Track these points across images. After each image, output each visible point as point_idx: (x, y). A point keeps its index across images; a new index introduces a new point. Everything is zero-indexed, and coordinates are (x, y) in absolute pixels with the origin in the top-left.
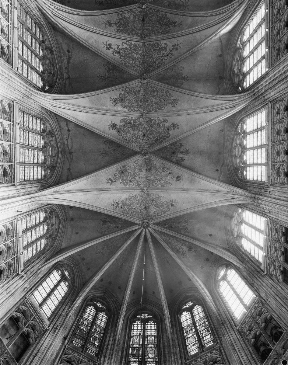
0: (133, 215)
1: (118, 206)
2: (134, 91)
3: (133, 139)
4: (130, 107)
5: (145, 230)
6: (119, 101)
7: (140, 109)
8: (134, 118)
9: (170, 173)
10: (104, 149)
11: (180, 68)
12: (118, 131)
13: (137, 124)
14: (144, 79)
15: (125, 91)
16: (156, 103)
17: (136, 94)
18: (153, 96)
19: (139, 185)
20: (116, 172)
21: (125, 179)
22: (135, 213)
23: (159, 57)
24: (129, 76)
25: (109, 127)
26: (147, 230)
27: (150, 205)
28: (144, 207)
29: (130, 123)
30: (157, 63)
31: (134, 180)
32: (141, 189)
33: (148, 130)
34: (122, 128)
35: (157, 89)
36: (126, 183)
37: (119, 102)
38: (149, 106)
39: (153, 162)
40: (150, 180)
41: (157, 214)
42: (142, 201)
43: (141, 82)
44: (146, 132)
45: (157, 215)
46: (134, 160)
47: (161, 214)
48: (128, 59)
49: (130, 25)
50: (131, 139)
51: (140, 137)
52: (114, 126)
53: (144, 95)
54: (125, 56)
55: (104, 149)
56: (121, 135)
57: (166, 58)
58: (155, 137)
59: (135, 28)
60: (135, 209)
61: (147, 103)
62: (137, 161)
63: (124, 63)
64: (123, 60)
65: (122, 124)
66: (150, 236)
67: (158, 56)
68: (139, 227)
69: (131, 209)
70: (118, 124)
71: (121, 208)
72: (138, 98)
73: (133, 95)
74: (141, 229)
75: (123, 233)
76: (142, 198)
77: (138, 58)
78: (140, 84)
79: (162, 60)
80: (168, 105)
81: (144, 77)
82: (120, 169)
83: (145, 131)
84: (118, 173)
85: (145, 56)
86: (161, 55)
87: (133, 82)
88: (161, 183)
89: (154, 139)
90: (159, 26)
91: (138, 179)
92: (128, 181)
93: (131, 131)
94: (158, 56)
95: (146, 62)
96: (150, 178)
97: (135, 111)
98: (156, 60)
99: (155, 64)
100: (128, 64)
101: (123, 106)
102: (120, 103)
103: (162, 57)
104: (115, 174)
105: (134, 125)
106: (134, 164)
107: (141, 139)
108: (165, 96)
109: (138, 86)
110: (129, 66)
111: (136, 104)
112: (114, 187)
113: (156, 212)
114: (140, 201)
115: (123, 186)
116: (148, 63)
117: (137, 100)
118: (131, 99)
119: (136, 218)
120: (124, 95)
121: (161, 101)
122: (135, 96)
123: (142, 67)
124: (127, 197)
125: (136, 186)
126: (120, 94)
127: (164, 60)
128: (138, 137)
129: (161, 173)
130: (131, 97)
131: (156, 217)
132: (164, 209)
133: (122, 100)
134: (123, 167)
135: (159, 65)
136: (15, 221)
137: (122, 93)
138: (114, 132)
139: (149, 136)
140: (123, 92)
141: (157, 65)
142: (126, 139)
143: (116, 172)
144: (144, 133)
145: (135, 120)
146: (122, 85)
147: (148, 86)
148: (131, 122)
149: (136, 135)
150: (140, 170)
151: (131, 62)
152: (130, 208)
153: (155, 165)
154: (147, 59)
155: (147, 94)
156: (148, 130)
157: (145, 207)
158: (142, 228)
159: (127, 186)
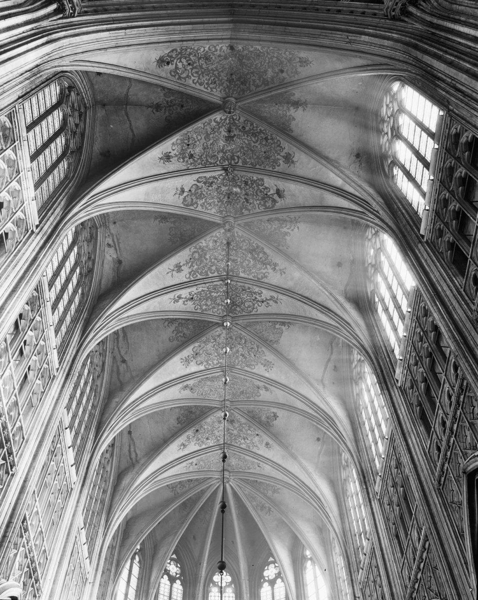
7: (221, 361)
9: (257, 435)
16: (243, 355)
17: (215, 340)
18: (239, 344)
36: (202, 442)
40: (232, 434)
49: (207, 257)
57: (260, 304)
59: (215, 259)
72: (219, 344)
79: (254, 305)
80: (259, 364)
88: (246, 442)
90: (251, 260)
92: (205, 440)
96: (232, 432)
100: (204, 307)
101: (198, 363)
103: (254, 300)
111: (216, 354)
116: (234, 301)
122: (214, 343)
129: (247, 431)
133: (196, 354)
136: (13, 111)
142: (202, 394)
151: (209, 303)
155: (231, 338)
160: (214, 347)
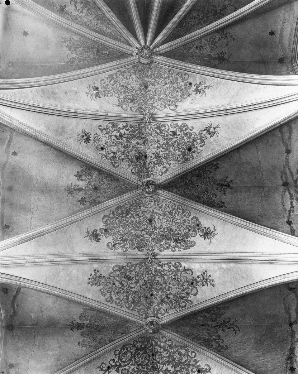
0: (169, 71)
1: (197, 87)
2: (171, 302)
3: (171, 213)
4: (178, 271)
5: (146, 43)
6: (198, 282)
7: (158, 268)
8: (170, 250)
9: (102, 149)
10: (225, 194)
11: (86, 343)
12: (198, 225)
13: (164, 241)
14: (152, 323)
15: (188, 301)
16: (130, 279)
17: (167, 297)
18: (135, 293)
19: (158, 128)
20: (201, 148)
21: (185, 138)
22: (166, 75)
23: (126, 365)
24: (179, 330)
25: (216, 232)
26: (143, 43)
27: (138, 92)
28: (149, 88)
29: (177, 241)
30: (129, 354)
31: (167, 136)
32: (154, 119)
33: (143, 230)
34: (191, 232)
35: (128, 306)
36: (182, 130)
37: (198, 280)
38: (142, 274)
39: (133, 171)
40: (139, 138)
41: (125, 74)
42: (152, 98)
43: (158, 318)
44: (147, 226)
45: (124, 72)
46: (168, 173)
47: (118, 75)
48: (182, 361)
50: (174, 212)
51: (157, 217)
52: (207, 234)
53: (152, 295)
54: (189, 365)
55: (225, 194)
56: (192, 219)
57: (112, 362)
58: (130, 217)
60: (166, 84)
61: (146, 279)
62: (162, 173)
63: (190, 353)
64: (192, 358)
65: (192, 239)
66: (137, 31)
67: (127, 367)
68: (157, 49)
69: (172, 83)
70: (198, 239)
71: (190, 84)
72: (162, 289)
73: (172, 294)
74: (153, 44)
75: (187, 36)
76: (152, 104)
77: (165, 364)
78: (160, 316)
79: (119, 359)
80: (107, 275)
81: (152, 327)
82: (195, 155)
83: (149, 228)
84: (197, 147)
85: (150, 366)
86: (121, 369)
87: (172, 317)
88: (119, 131)
89: (133, 214)
91: (161, 139)
92: (178, 133)
93: (174, 228)
94: (127, 367)
95: (149, 356)
96: (139, 141)
97: (168, 264)
98: (130, 360)
99: (131, 352)
100: (183, 351)
101: (190, 272)
102: (196, 277)
103: (120, 366)
104: (204, 145)
105: (170, 239)
106: (168, 166)
107: (157, 213)
108: (113, 293)
109: (163, 312)
110: (181, 349)
111: (165, 277)
112: (204, 120)
113: (127, 78)
114: (156, 98)
115: (187, 122)
116: (145, 355)
117: (164, 286)
118: (176, 286)
119: (164, 67)
120: (188, 294)
121: (121, 283)
122: (168, 292)
123: (156, 347)
124: (180, 104)
125: (164, 125)
126: (195, 295)
127: (116, 360)
128: (161, 218)
129: (118, 150)
130: (175, 290)
131: (127, 69)
132: (112, 82)
133: (192, 283)
134: (188, 160)
135: (125, 350)
137: (192, 296)
138: (206, 223)
139: (142, 220)
140: (191, 298)
141: (128, 351)
142: (183, 211)
143: (201, 148)
144: (151, 224)
145: (168, 248)
146: (193, 309)
147: (145, 311)
148: (174, 244)
149: (165, 220)
150: (157, 156)
152: (175, 85)
153: (129, 166)
154: (147, 361)
155: (146, 298)
156: (143, 230)
157: (146, 87)
158: (151, 46)
159: (180, 123)
160: (169, 287)
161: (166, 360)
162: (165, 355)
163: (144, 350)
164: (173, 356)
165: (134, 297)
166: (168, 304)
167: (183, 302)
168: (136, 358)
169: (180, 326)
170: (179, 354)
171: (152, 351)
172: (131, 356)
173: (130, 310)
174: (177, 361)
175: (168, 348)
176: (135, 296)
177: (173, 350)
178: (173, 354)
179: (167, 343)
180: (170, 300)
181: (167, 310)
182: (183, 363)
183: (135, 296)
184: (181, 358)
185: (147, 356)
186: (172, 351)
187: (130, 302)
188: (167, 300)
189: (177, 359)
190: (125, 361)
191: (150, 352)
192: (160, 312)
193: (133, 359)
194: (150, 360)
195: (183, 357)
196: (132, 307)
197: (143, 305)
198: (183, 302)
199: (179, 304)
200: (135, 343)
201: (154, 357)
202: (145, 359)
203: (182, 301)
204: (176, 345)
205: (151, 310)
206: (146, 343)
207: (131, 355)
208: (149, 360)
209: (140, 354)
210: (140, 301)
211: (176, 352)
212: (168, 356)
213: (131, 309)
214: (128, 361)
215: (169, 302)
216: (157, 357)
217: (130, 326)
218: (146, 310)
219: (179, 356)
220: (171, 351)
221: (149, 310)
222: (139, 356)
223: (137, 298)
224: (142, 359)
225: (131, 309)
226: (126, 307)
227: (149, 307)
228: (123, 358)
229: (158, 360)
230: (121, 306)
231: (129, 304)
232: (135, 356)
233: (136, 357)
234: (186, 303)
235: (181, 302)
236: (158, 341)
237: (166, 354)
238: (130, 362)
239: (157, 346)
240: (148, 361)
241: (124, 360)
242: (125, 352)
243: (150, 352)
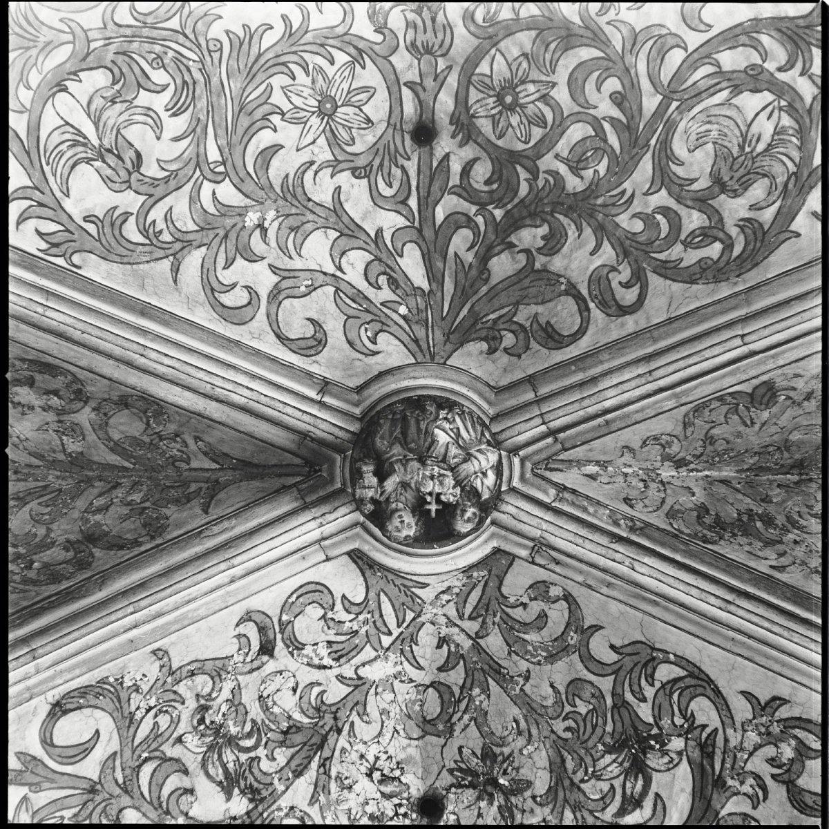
2: (219, 739)
23: (734, 37)
24: (125, 425)
35: (704, 710)
43: (357, 557)
48: (99, 79)
95: (464, 126)
99: (663, 177)
109: (308, 625)
110: (114, 221)
123: (390, 221)
135: (734, 209)
141: (702, 202)
147: (511, 629)
154: (495, 67)
161: (279, 81)
162: (287, 134)
163: (524, 189)
164: (196, 131)
165: (634, 803)
166: (255, 712)
167: (85, 749)
168: (616, 113)
169: (114, 459)
170: (129, 155)
171: (436, 174)
172: (665, 144)
173: (681, 661)
174: (159, 77)
175: (252, 218)
176: (622, 812)
177: (194, 199)
178: (199, 161)
179: (265, 281)
180: (229, 756)
181: (267, 649)
182: (84, 62)
183: (622, 812)
184: (112, 115)
185: (485, 125)
186: (207, 187)
187: (677, 744)
188: (261, 752)
189: (160, 102)
190: (737, 90)
191: (456, 167)
192: (341, 615)
193: (651, 102)
194: (453, 80)
195: (89, 129)
196: (649, 692)
197: (523, 701)
198: (85, 749)
199: (128, 722)
200: (627, 285)
201: (409, 108)
202: (510, 86)
203: (90, 768)
204: (166, 265)
205: (443, 641)
206: (502, 266)
207: (665, 155)
208: (467, 79)
209: (563, 147)
210: (559, 745)
211: (170, 182)
212: (250, 133)
213: (665, 672)
214: (711, 91)
215: (232, 741)
216: (378, 108)
217: (679, 464)
218: (494, 643)
219: (133, 133)
220: (228, 193)
221: (467, 644)
222: (577, 132)
223: (593, 789)
224: (544, 98)
225: (665, 672)
226: (717, 697)
227: (456, 677)
228: (765, 128)
229: (370, 75)
230: (784, 713)
231: (691, 727)
232: (627, 129)
233: (613, 121)
234: (47, 742)
235: (100, 753)
236: (362, 285)
237: (277, 148)
238: (678, 76)
239: (379, 232)
240: (484, 68)
241: (751, 102)
242: (735, 194)
243: (456, 167)
